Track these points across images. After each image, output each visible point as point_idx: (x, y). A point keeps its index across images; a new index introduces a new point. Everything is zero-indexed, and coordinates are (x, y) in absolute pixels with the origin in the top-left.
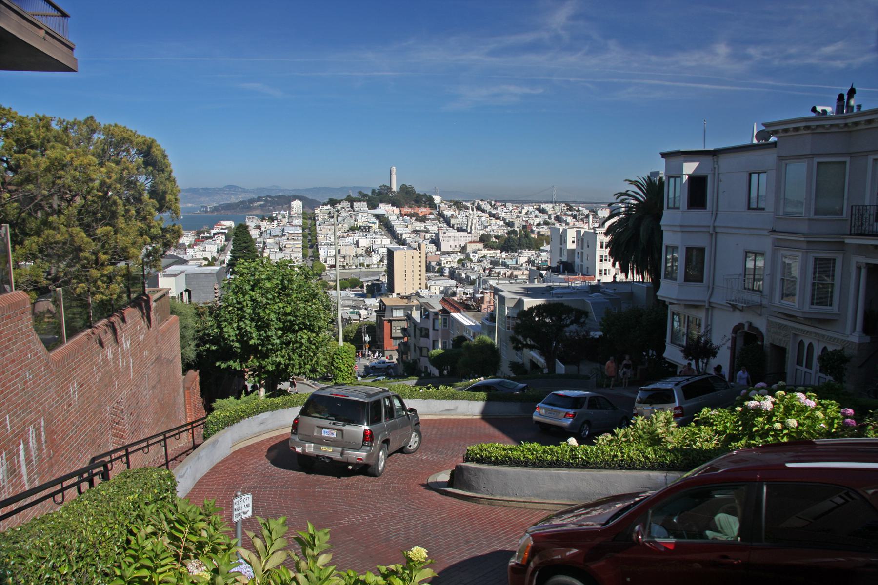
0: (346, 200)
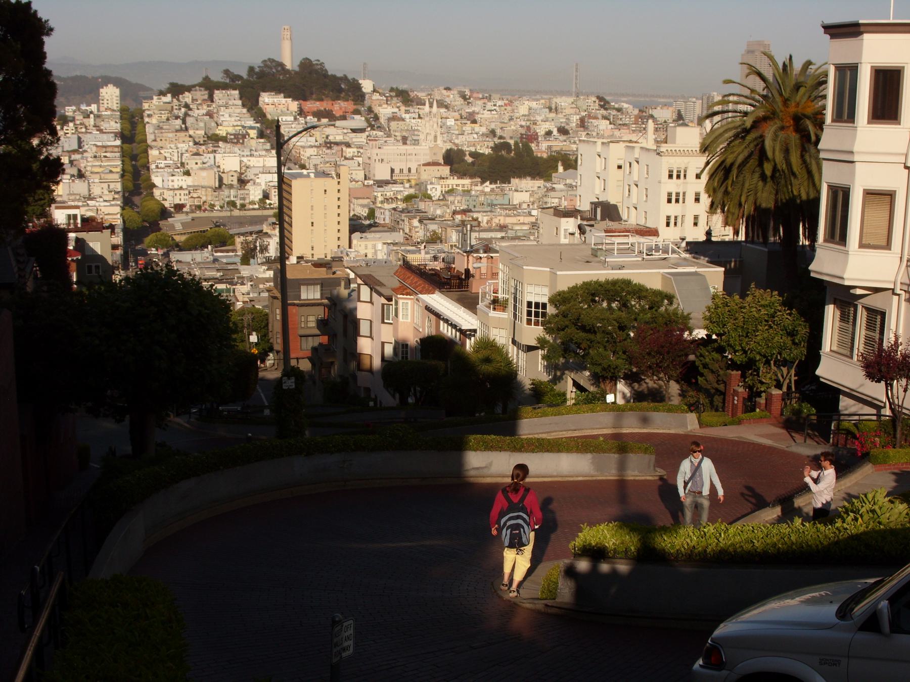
0: (200, 85)
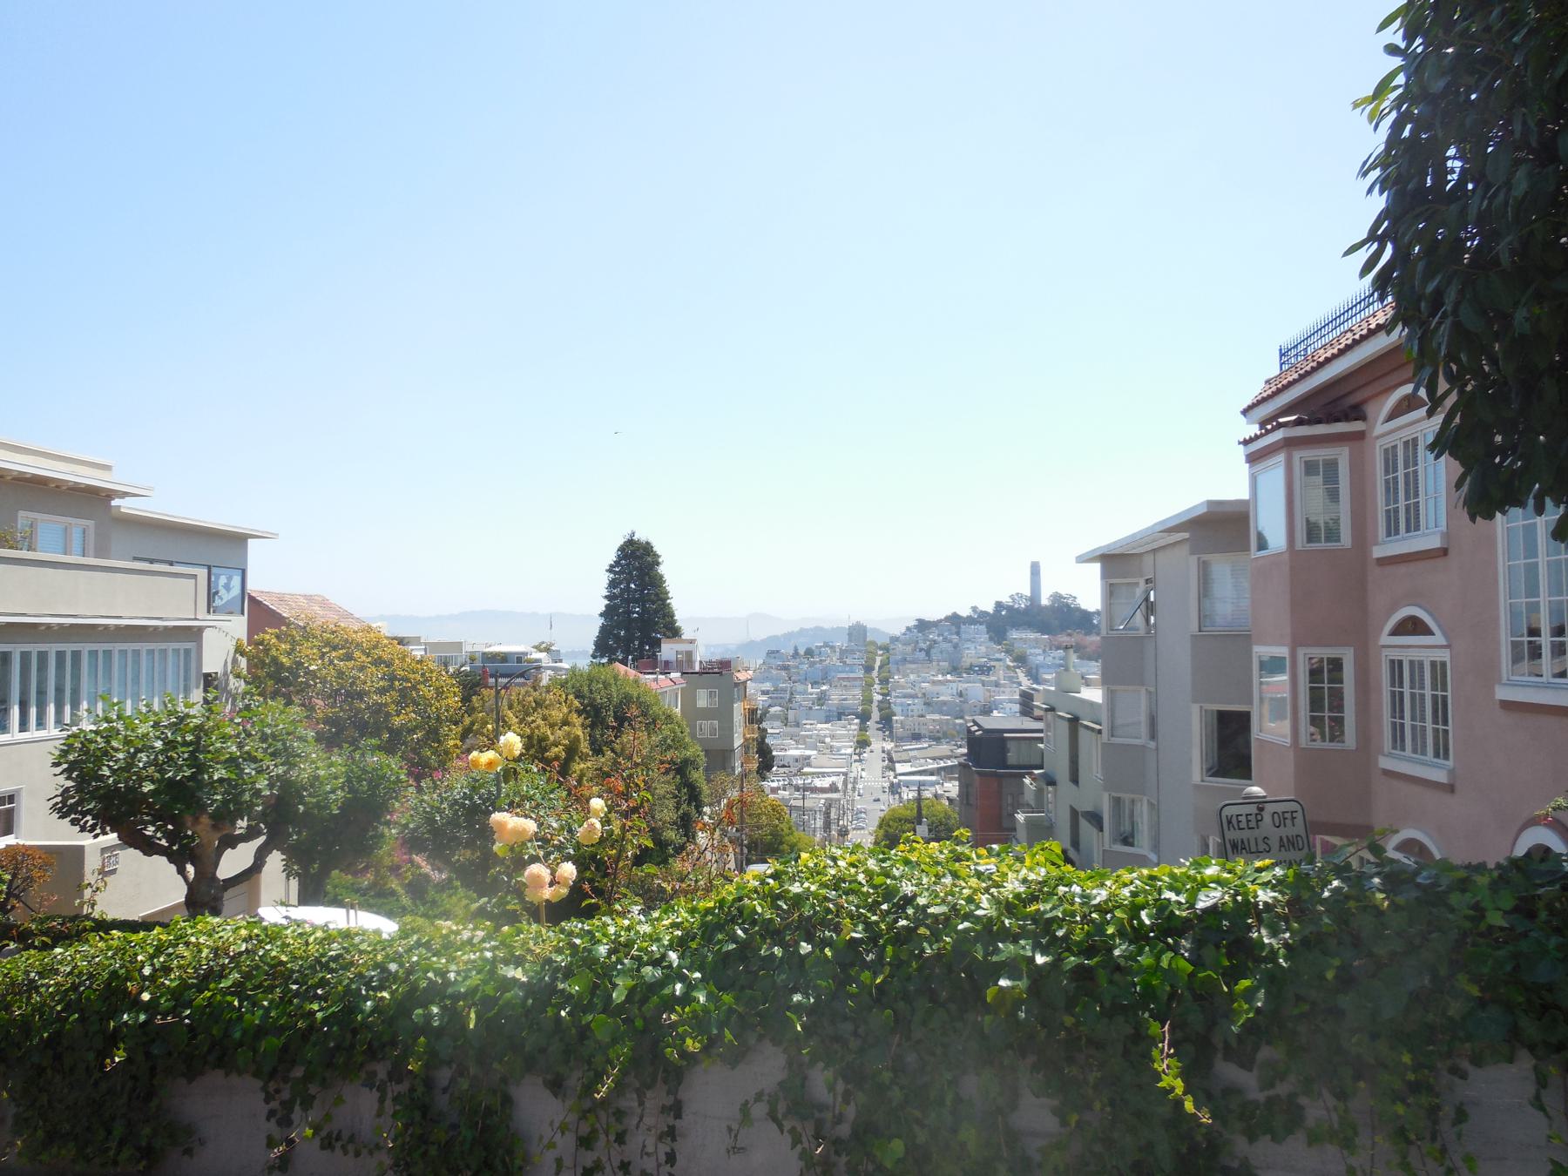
0: (947, 619)
